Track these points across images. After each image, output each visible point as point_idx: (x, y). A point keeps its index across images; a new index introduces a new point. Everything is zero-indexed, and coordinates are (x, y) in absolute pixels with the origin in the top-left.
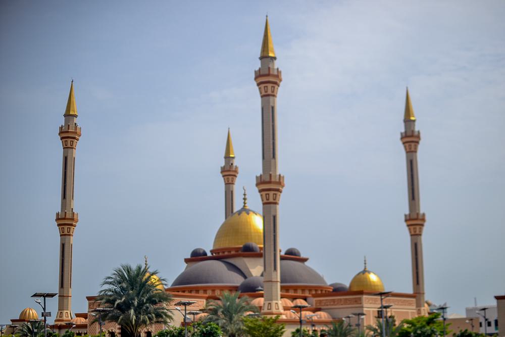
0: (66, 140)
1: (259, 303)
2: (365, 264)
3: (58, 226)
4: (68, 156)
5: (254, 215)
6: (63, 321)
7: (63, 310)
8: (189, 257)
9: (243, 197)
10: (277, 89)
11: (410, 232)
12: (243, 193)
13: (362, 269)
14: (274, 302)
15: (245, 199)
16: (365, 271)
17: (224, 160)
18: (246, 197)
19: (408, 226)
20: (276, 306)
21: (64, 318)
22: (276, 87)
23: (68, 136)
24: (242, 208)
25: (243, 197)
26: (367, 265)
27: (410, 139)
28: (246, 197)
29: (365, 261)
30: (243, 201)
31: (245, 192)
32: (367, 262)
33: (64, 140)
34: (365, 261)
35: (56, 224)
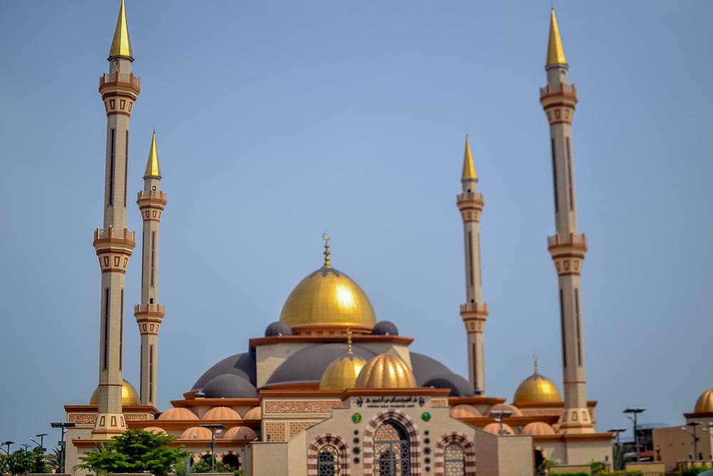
0: (124, 99)
1: (254, 415)
2: (536, 366)
3: (97, 254)
4: (115, 128)
5: (334, 276)
6: (106, 433)
7: (107, 412)
8: (262, 335)
9: (324, 250)
10: (573, 113)
11: (467, 329)
12: (324, 244)
13: (531, 373)
14: (571, 410)
15: (326, 254)
16: (536, 376)
17: (143, 181)
18: (329, 250)
19: (465, 320)
20: (573, 416)
21: (108, 427)
22: (571, 110)
23: (114, 93)
24: (322, 268)
25: (324, 250)
26: (538, 368)
27: (468, 206)
28: (329, 250)
29: (536, 362)
30: (325, 256)
31: (326, 243)
32: (538, 363)
33: (108, 99)
34: (536, 362)
35: (94, 250)
